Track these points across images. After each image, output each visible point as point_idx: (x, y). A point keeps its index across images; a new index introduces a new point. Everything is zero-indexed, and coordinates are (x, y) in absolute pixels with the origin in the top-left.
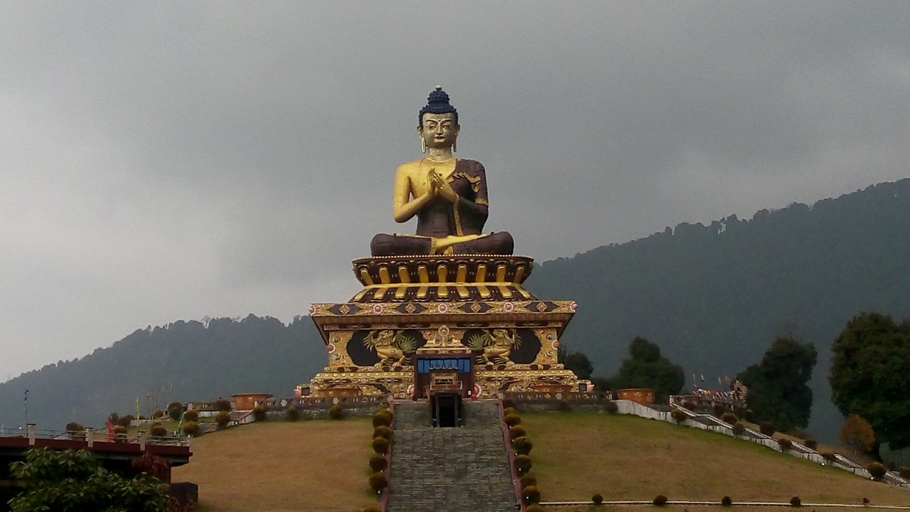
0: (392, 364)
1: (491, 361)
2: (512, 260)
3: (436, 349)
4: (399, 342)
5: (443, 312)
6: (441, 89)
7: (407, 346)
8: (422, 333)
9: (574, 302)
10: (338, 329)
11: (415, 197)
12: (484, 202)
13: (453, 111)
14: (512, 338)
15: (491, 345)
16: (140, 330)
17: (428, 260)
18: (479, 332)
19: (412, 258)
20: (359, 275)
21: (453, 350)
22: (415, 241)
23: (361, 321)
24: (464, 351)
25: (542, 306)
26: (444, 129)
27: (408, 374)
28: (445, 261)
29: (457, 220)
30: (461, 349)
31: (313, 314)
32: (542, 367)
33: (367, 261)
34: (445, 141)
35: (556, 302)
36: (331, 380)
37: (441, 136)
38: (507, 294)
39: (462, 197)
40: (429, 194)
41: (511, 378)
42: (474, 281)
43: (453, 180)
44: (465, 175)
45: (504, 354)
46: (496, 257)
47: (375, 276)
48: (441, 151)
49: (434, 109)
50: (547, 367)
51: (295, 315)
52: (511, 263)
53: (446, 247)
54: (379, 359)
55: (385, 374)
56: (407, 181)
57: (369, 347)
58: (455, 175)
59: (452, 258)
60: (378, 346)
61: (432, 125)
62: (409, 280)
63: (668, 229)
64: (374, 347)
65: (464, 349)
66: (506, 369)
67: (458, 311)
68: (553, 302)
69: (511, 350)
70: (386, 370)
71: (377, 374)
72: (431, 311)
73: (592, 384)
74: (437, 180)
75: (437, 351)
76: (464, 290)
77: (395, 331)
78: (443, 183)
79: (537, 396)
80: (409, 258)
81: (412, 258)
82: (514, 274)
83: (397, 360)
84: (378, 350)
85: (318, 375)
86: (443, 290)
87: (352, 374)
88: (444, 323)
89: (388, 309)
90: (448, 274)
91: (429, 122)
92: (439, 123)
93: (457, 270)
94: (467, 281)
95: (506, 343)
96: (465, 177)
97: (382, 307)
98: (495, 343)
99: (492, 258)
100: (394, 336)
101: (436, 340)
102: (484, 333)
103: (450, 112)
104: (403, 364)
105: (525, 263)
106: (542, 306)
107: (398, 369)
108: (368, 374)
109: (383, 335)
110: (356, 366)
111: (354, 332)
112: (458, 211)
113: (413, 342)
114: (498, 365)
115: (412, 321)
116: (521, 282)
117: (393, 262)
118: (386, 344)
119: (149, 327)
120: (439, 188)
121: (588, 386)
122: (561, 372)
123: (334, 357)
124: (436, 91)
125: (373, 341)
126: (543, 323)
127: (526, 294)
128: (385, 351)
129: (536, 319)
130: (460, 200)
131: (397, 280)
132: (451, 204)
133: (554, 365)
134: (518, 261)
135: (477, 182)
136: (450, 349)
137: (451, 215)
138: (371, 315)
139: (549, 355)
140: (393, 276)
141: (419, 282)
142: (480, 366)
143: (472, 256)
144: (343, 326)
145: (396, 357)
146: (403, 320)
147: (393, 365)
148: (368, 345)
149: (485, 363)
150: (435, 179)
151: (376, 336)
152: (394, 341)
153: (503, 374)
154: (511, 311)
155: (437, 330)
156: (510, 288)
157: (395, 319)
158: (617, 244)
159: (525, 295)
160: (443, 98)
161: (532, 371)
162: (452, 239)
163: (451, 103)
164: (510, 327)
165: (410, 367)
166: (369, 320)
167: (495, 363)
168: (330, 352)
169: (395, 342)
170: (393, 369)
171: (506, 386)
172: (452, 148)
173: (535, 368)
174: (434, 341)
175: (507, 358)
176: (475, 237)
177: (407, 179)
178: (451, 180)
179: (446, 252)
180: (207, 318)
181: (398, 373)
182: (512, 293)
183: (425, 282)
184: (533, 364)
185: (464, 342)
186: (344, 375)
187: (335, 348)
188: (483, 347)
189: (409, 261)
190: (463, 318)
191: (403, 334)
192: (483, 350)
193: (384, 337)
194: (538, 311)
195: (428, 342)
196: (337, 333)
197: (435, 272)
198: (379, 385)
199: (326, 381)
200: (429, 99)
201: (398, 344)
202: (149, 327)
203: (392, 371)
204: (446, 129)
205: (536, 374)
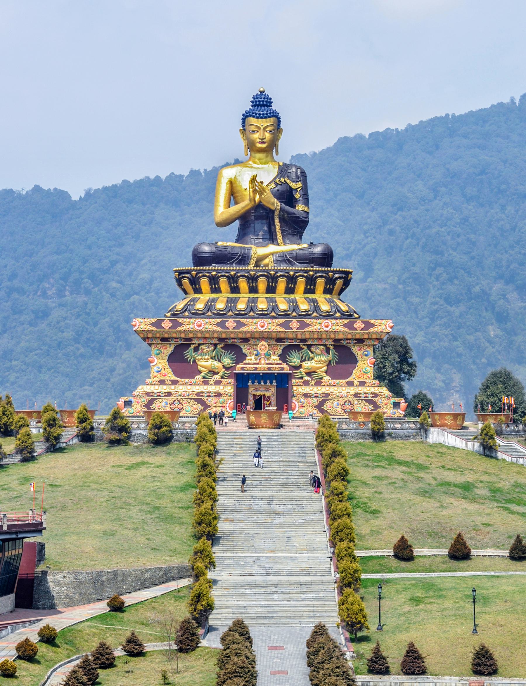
0: (212, 376)
1: (307, 376)
2: (331, 274)
3: (255, 366)
4: (220, 355)
5: (262, 329)
6: (264, 92)
7: (227, 361)
8: (242, 347)
9: (391, 321)
10: (159, 342)
11: (236, 203)
12: (306, 209)
13: (276, 116)
14: (329, 354)
15: (309, 360)
17: (249, 272)
18: (298, 348)
19: (233, 270)
20: (180, 284)
21: (271, 368)
22: (236, 251)
23: (183, 335)
24: (283, 369)
25: (359, 325)
30: (280, 366)
31: (136, 328)
32: (357, 383)
33: (188, 272)
34: (267, 147)
35: (372, 321)
36: (153, 393)
37: (264, 141)
38: (325, 307)
39: (283, 205)
40: (250, 200)
41: (328, 395)
42: (293, 293)
43: (274, 186)
44: (286, 180)
45: (321, 370)
47: (195, 286)
49: (256, 114)
50: (362, 384)
51: (86, 189)
52: (331, 276)
53: (266, 256)
54: (200, 372)
55: (205, 387)
56: (228, 185)
57: (190, 360)
58: (277, 181)
59: (273, 270)
60: (198, 360)
62: (229, 290)
63: (512, 100)
64: (194, 361)
65: (282, 366)
66: (322, 384)
67: (277, 328)
68: (370, 321)
69: (328, 365)
70: (206, 382)
71: (197, 387)
72: (251, 327)
73: (405, 402)
75: (256, 369)
76: (283, 302)
77: (215, 345)
79: (351, 425)
80: (230, 270)
82: (333, 287)
83: (217, 373)
84: (199, 363)
85: (140, 387)
86: (262, 302)
87: (173, 387)
88: (263, 339)
90: (268, 286)
92: (262, 128)
94: (286, 293)
95: (323, 359)
96: (287, 183)
97: (203, 322)
98: (313, 359)
99: (313, 271)
100: (214, 350)
101: (256, 355)
102: (303, 349)
103: (273, 116)
104: (222, 378)
105: (344, 276)
106: (359, 325)
107: (218, 383)
108: (189, 387)
109: (204, 349)
110: (177, 379)
111: (176, 345)
113: (233, 355)
114: (315, 380)
115: (232, 336)
116: (340, 293)
117: (214, 273)
118: (206, 357)
120: (260, 195)
121: (401, 405)
122: (376, 388)
123: (156, 369)
125: (193, 354)
126: (360, 341)
127: (344, 307)
129: (354, 337)
130: (281, 207)
132: (273, 212)
133: (370, 381)
136: (269, 366)
137: (272, 222)
138: (192, 330)
139: (364, 370)
140: (213, 286)
141: (240, 293)
142: (297, 380)
143: (291, 269)
144: (164, 340)
145: (216, 371)
146: (224, 336)
147: (213, 378)
148: (188, 358)
149: (302, 378)
150: (256, 187)
151: (196, 349)
152: (214, 355)
153: (320, 390)
154: (329, 329)
155: (257, 345)
156: (330, 301)
157: (216, 335)
158: (453, 116)
159: (344, 308)
160: (266, 102)
161: (348, 388)
162: (272, 248)
163: (274, 107)
164: (327, 343)
165: (230, 381)
166: (191, 335)
167: (312, 378)
168: (151, 364)
169: (215, 356)
170: (212, 382)
171: (322, 403)
172: (274, 150)
173: (350, 384)
174: (253, 357)
175: (324, 374)
176: (295, 247)
178: (273, 185)
179: (266, 261)
181: (217, 386)
182: (330, 305)
183: (246, 293)
184: (349, 379)
185: (283, 357)
186: (165, 387)
187: (156, 360)
188: (301, 362)
190: (282, 336)
191: (222, 348)
192: (301, 365)
193: (205, 351)
194: (356, 329)
195: (248, 358)
196: (159, 346)
198: (199, 399)
199: (148, 394)
200: (252, 102)
201: (218, 358)
203: (211, 384)
205: (352, 390)
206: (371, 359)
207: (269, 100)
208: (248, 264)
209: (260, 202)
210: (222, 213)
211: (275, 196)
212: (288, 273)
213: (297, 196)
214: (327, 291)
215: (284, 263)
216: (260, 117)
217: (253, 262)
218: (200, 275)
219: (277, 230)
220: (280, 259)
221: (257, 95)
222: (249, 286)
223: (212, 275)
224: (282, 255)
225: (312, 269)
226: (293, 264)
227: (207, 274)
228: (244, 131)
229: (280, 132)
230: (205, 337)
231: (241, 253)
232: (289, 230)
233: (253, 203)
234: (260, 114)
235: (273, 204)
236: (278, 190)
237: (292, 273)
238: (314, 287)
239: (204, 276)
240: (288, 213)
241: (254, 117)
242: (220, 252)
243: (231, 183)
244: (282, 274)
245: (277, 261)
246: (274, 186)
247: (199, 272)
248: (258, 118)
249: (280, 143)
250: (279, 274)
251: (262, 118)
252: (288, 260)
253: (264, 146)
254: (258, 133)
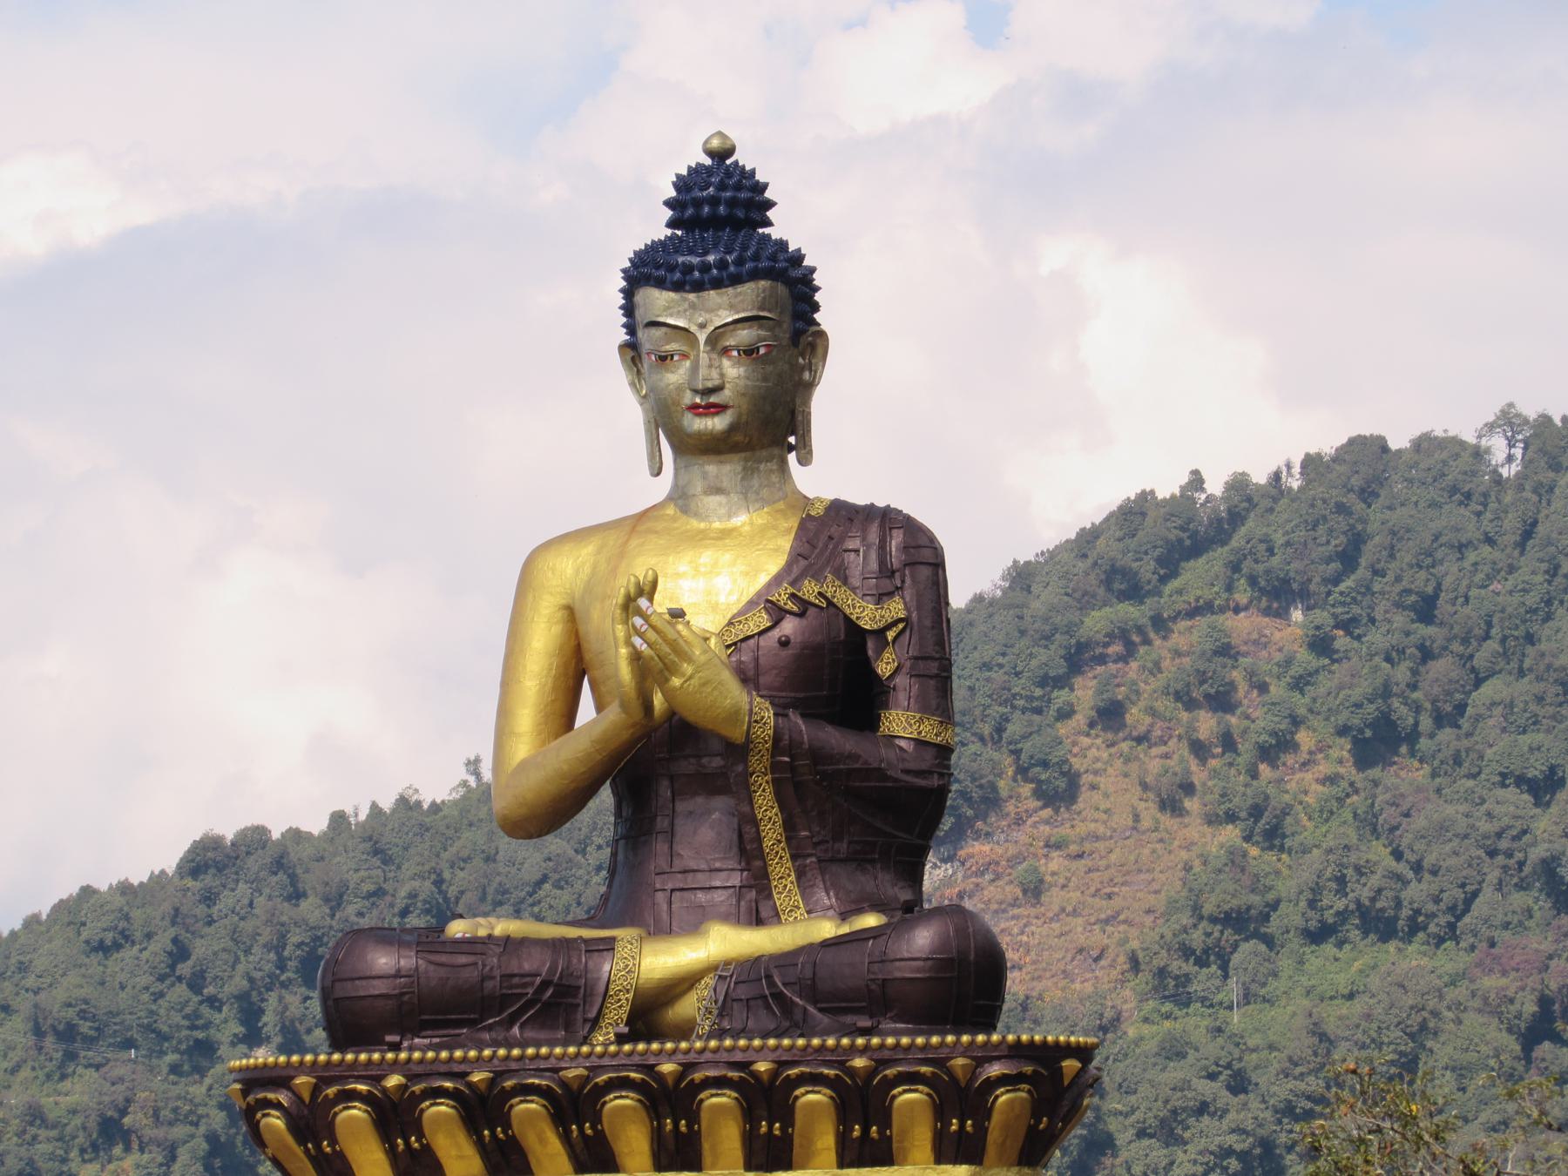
12: (929, 730)
16: (1145, 497)
22: (531, 963)
26: (726, 363)
28: (633, 1075)
29: (772, 834)
34: (733, 428)
37: (713, 399)
40: (624, 706)
43: (765, 621)
46: (882, 1046)
47: (318, 1147)
48: (727, 468)
49: (672, 268)
52: (959, 1073)
56: (557, 629)
58: (782, 597)
61: (668, 347)
74: (650, 645)
78: (685, 656)
80: (465, 1060)
82: (982, 1131)
91: (657, 333)
92: (702, 337)
93: (694, 1117)
96: (830, 603)
99: (866, 1050)
103: (754, 275)
105: (1028, 1069)
112: (776, 783)
117: (393, 1081)
119: (1197, 480)
124: (708, 161)
132: (738, 751)
134: (991, 1060)
135: (889, 627)
160: (732, 203)
177: (566, 613)
179: (689, 1006)
180: (1508, 420)
189: (467, 1074)
197: (593, 1127)
200: (669, 204)
202: (1197, 480)
204: (738, 363)
207: (743, 195)
208: (595, 1023)
209: (671, 714)
210: (524, 764)
211: (748, 677)
212: (744, 1066)
213: (884, 667)
215: (763, 1013)
216: (687, 282)
217: (617, 1015)
218: (331, 1091)
219: (767, 843)
220: (743, 992)
221: (696, 171)
222: (566, 1138)
223: (384, 1090)
224: (753, 976)
225: (860, 1041)
226: (798, 1016)
227: (362, 1087)
228: (632, 351)
229: (813, 347)
231: (552, 969)
232: (837, 838)
233: (638, 714)
234: (688, 269)
235: (734, 716)
236: (784, 643)
237: (762, 1067)
238: (881, 1132)
239: (349, 1096)
240: (818, 756)
241: (660, 284)
242: (442, 972)
243: (572, 616)
244: (712, 1073)
245: (725, 1008)
246: (765, 621)
247: (326, 1074)
248: (678, 287)
250: (698, 1076)
251: (698, 287)
252: (778, 996)
253: (717, 423)
254: (688, 363)
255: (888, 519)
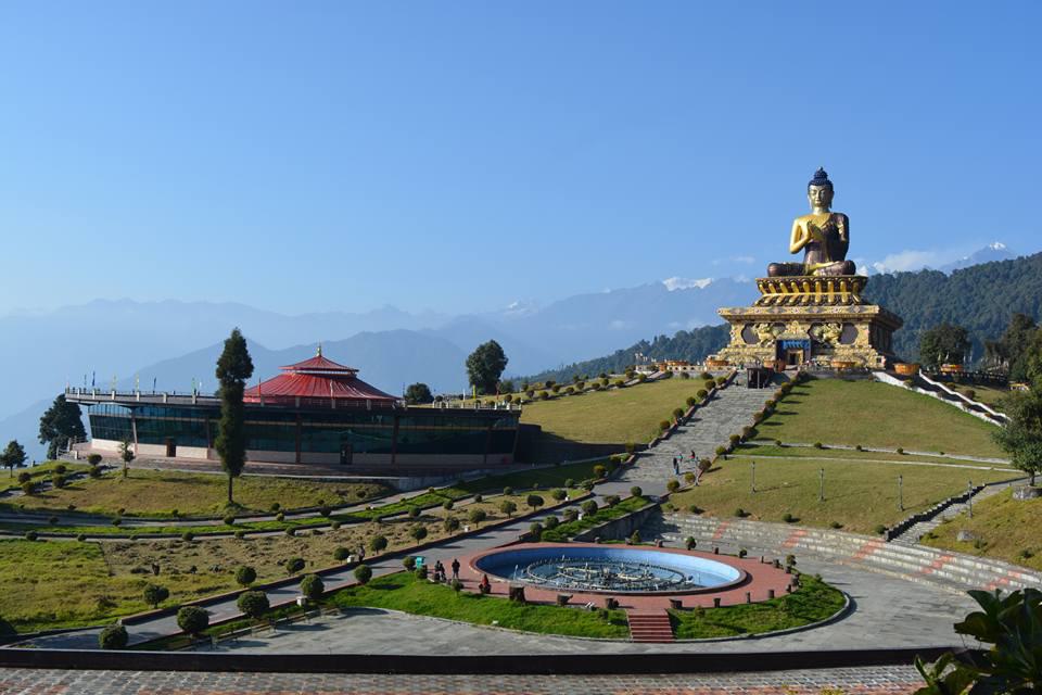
27: (773, 350)
50: (860, 347)
81: (787, 278)
84: (760, 335)
89: (763, 311)
107: (770, 347)
116: (859, 291)
126: (860, 320)
128: (762, 336)
131: (780, 291)
151: (758, 327)
173: (853, 347)
205: (852, 351)
206: (867, 332)
214: (848, 290)
230: (762, 318)
249: (834, 201)
255: (842, 214)
